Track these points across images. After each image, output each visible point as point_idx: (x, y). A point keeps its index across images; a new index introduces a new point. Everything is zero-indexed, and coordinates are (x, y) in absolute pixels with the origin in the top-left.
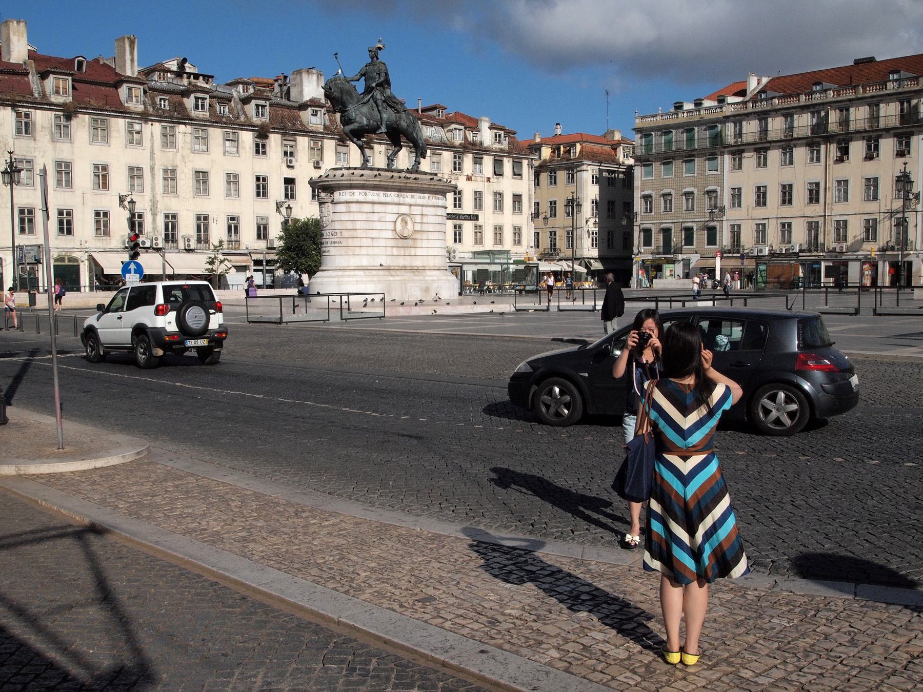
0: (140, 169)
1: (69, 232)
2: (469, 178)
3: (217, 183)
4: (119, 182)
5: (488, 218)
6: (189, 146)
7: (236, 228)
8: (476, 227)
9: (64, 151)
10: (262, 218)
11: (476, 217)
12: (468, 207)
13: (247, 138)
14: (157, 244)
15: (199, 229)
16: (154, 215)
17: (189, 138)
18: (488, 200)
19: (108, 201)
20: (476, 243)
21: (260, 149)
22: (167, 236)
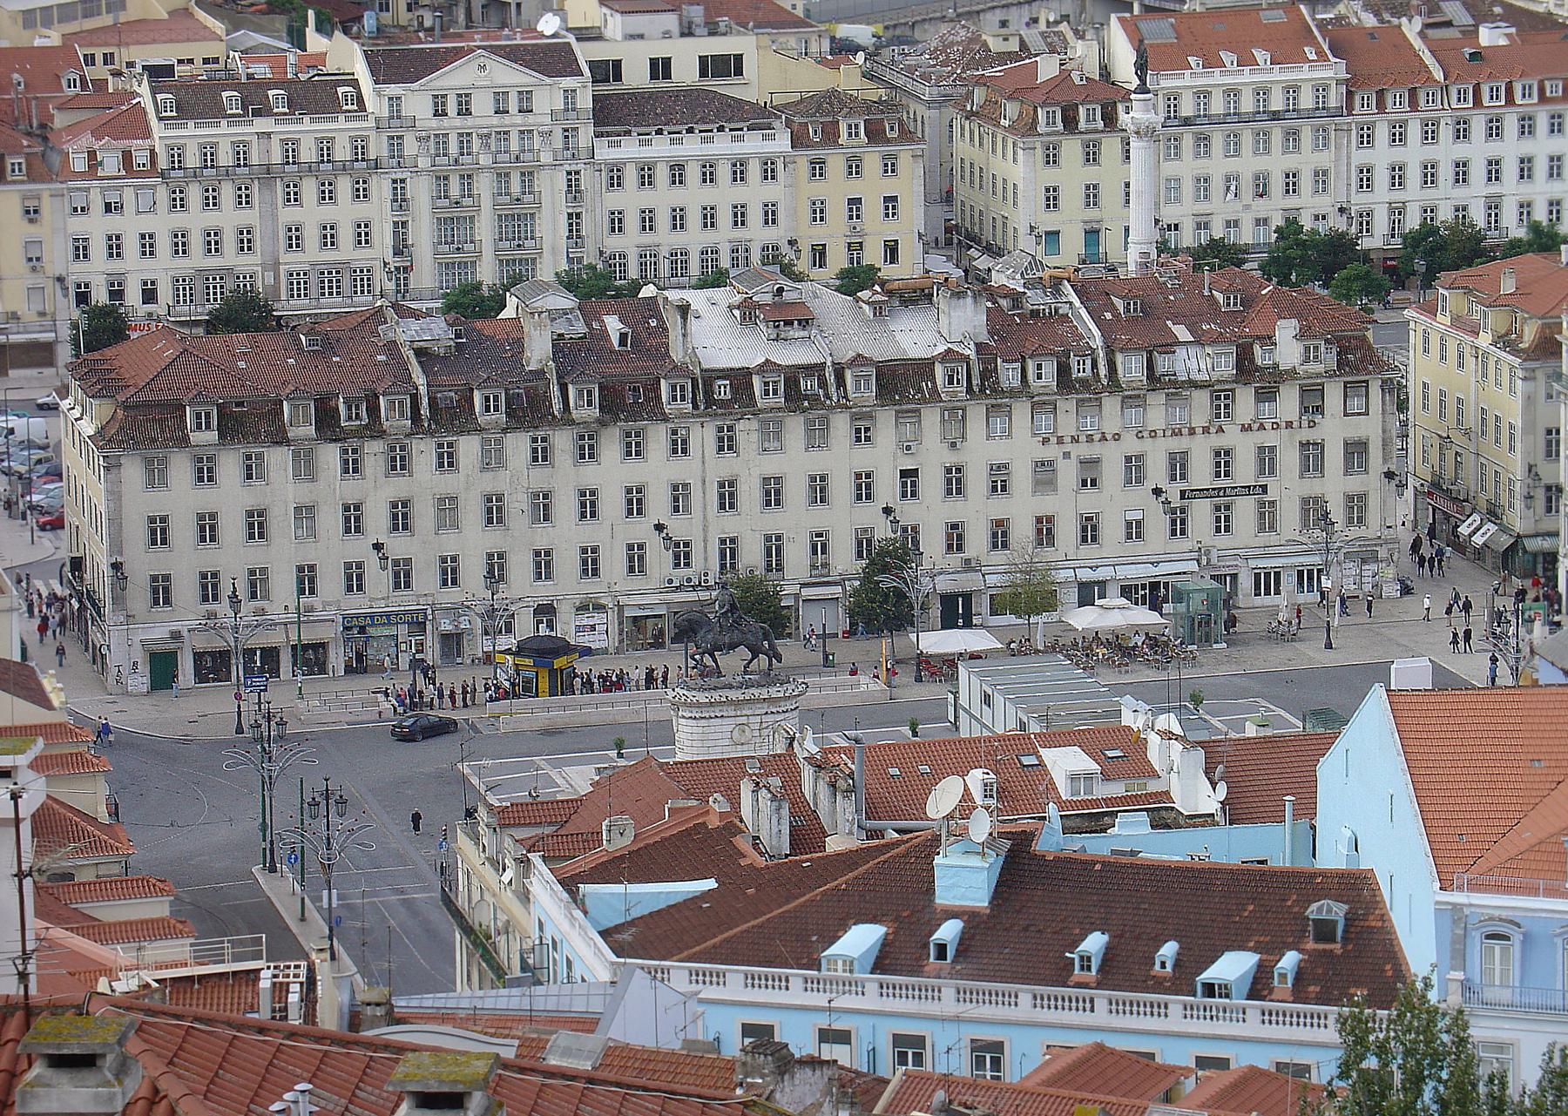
0: (686, 486)
1: (595, 573)
2: (1246, 428)
3: (796, 491)
4: (658, 505)
5: (1288, 488)
6: (755, 446)
7: (824, 546)
8: (1262, 504)
9: (590, 475)
10: (866, 530)
11: (1264, 488)
12: (1245, 471)
13: (841, 425)
14: (706, 581)
15: (769, 554)
16: (705, 541)
17: (755, 436)
18: (1289, 459)
19: (641, 529)
20: (1262, 529)
21: (862, 436)
22: (723, 566)
